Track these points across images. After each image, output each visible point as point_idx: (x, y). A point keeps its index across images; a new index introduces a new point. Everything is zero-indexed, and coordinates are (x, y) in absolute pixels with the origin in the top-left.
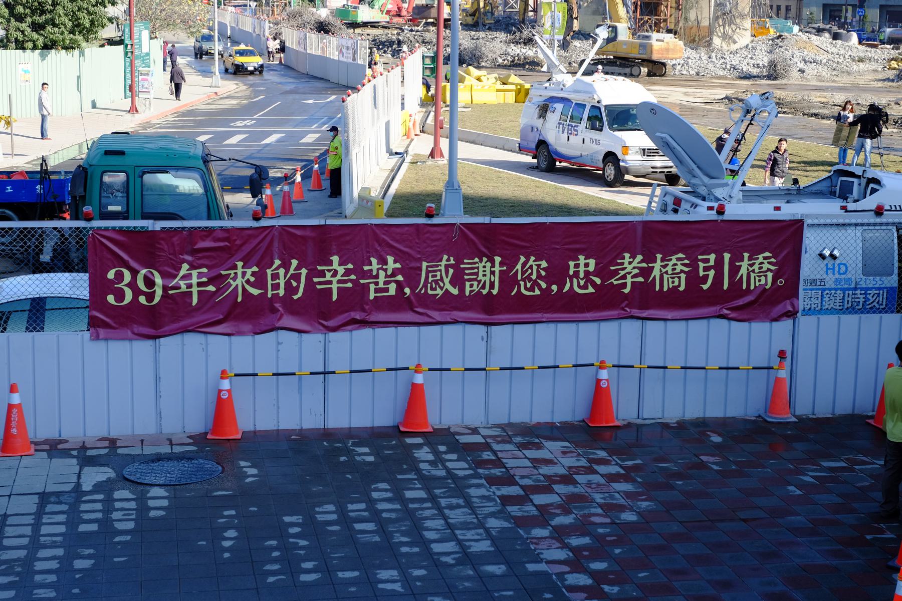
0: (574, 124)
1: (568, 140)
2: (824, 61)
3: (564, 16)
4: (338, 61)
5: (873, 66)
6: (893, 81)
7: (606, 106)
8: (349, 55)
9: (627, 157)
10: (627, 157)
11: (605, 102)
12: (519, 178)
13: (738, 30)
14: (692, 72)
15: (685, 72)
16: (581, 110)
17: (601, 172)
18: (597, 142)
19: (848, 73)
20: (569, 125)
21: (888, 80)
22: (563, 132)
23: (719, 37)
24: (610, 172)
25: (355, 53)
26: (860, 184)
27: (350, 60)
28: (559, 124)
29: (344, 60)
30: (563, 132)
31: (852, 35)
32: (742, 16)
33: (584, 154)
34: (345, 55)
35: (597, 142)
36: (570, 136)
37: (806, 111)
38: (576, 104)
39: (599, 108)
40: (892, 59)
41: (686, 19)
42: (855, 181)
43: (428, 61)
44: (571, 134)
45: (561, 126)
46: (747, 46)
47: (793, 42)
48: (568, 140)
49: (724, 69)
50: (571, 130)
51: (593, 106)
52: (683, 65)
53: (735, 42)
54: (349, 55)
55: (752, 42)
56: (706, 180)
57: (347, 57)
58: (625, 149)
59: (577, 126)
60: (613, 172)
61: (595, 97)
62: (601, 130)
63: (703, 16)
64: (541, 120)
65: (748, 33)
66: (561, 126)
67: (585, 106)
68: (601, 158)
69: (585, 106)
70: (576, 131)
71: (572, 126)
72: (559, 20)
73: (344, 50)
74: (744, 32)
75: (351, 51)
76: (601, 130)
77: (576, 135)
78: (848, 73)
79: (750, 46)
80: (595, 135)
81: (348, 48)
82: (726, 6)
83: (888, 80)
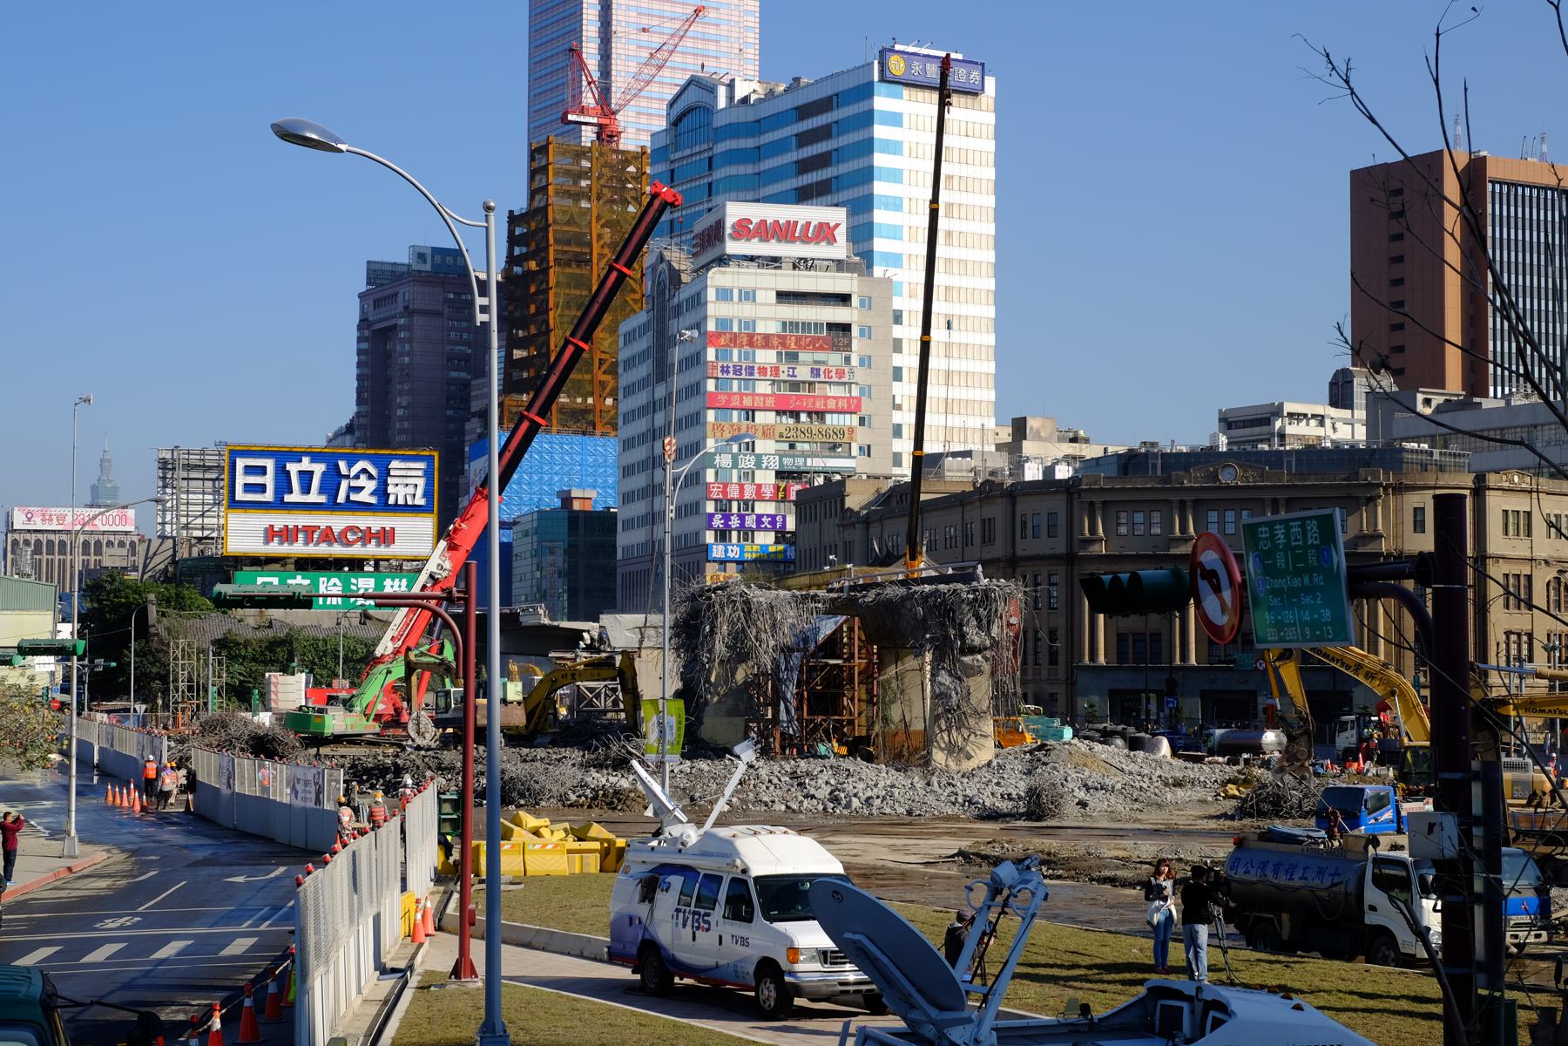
0: (702, 911)
1: (694, 939)
2: (1119, 786)
3: (680, 723)
4: (289, 807)
5: (1198, 793)
6: (1232, 818)
7: (757, 879)
8: (308, 796)
9: (799, 967)
10: (799, 967)
11: (757, 870)
12: (611, 1009)
13: (972, 738)
14: (901, 810)
15: (888, 810)
16: (715, 886)
17: (753, 994)
18: (744, 942)
19: (1160, 806)
20: (694, 913)
21: (1225, 816)
22: (684, 925)
23: (942, 749)
24: (769, 993)
25: (319, 792)
26: (1192, 1012)
27: (312, 805)
28: (678, 911)
29: (299, 803)
30: (684, 925)
31: (1160, 742)
32: (978, 714)
33: (721, 962)
34: (300, 795)
35: (744, 942)
36: (698, 933)
37: (1096, 874)
38: (705, 875)
39: (745, 882)
40: (1230, 781)
41: (886, 720)
42: (1185, 1005)
43: (447, 808)
44: (698, 928)
45: (681, 915)
46: (989, 764)
47: (1064, 755)
48: (694, 939)
49: (954, 804)
50: (698, 921)
51: (734, 880)
52: (884, 798)
53: (969, 757)
54: (308, 796)
55: (997, 756)
56: (934, 1013)
57: (305, 799)
58: (793, 952)
59: (708, 915)
60: (773, 994)
61: (738, 862)
62: (750, 920)
63: (914, 715)
64: (646, 906)
65: (990, 743)
66: (681, 915)
67: (721, 878)
68: (751, 969)
69: (721, 878)
70: (708, 922)
71: (699, 914)
72: (671, 728)
73: (299, 787)
74: (982, 741)
75: (313, 789)
76: (750, 920)
77: (708, 930)
78: (1160, 806)
79: (995, 764)
80: (739, 929)
81: (306, 783)
82: (951, 697)
83: (1225, 816)
